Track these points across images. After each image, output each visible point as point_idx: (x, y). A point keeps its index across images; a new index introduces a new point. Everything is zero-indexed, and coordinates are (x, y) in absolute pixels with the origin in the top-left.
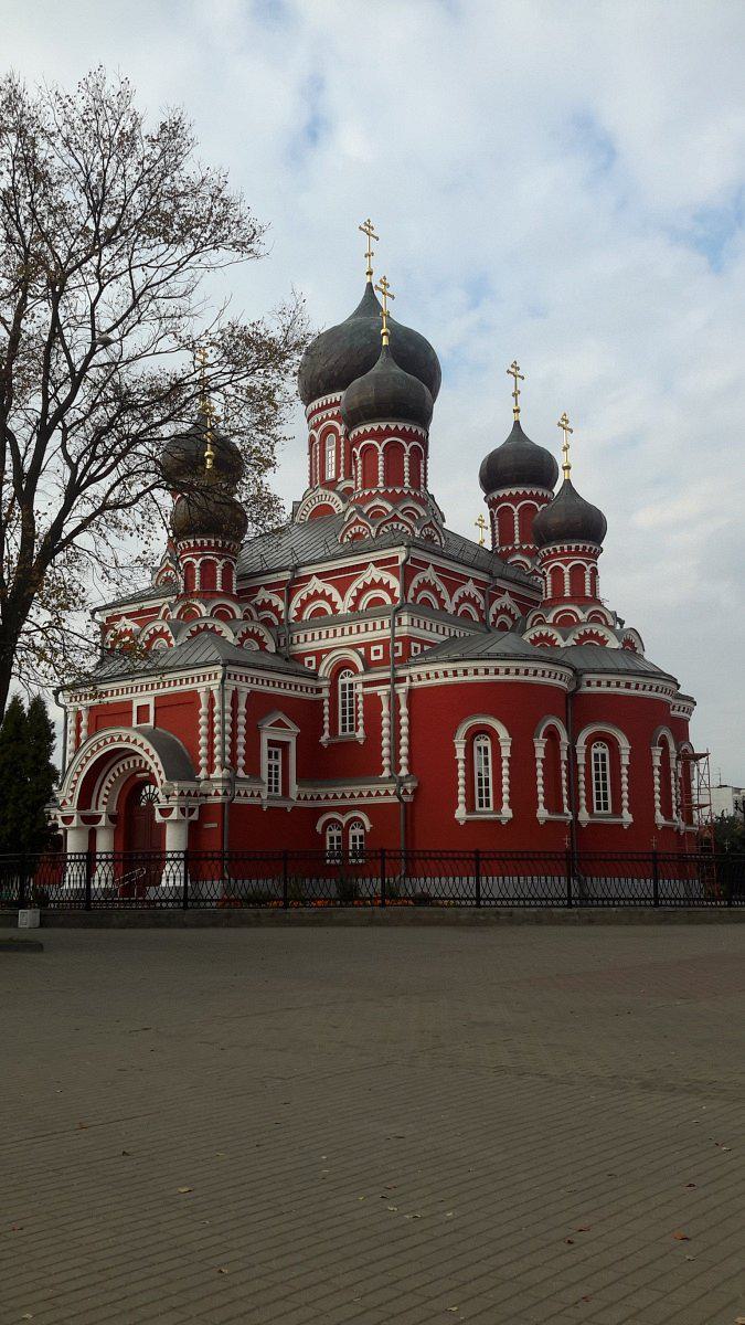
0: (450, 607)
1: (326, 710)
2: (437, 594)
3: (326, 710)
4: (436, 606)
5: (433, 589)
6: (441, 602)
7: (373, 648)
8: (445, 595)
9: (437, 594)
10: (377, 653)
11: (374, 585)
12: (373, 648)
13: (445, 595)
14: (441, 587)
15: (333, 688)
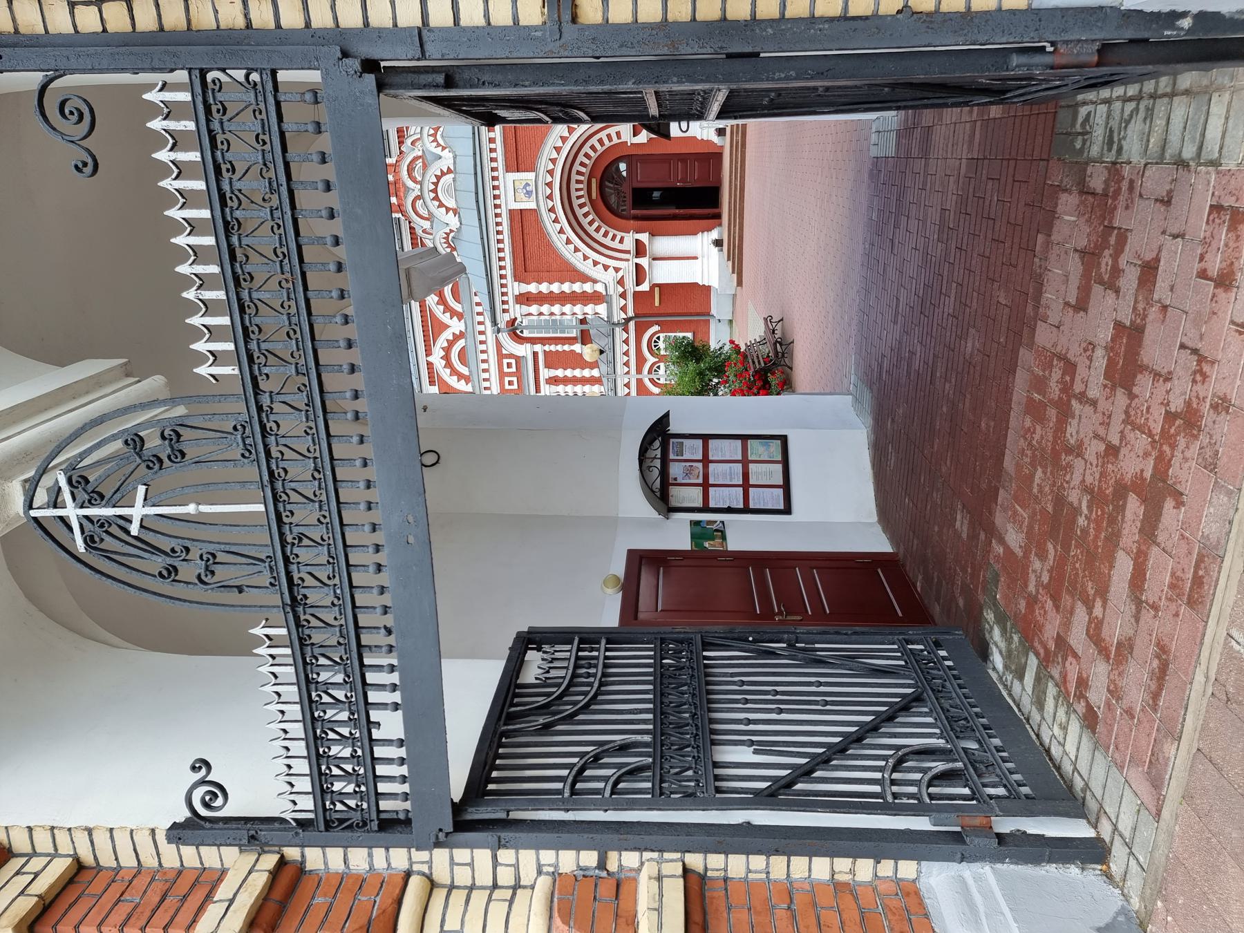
0: (456, 326)
1: (553, 348)
2: (451, 344)
3: (553, 348)
4: (461, 343)
5: (448, 350)
6: (457, 338)
7: (506, 370)
8: (447, 335)
9: (451, 344)
10: (509, 365)
11: (447, 358)
12: (506, 370)
13: (447, 335)
14: (442, 341)
15: (533, 341)
